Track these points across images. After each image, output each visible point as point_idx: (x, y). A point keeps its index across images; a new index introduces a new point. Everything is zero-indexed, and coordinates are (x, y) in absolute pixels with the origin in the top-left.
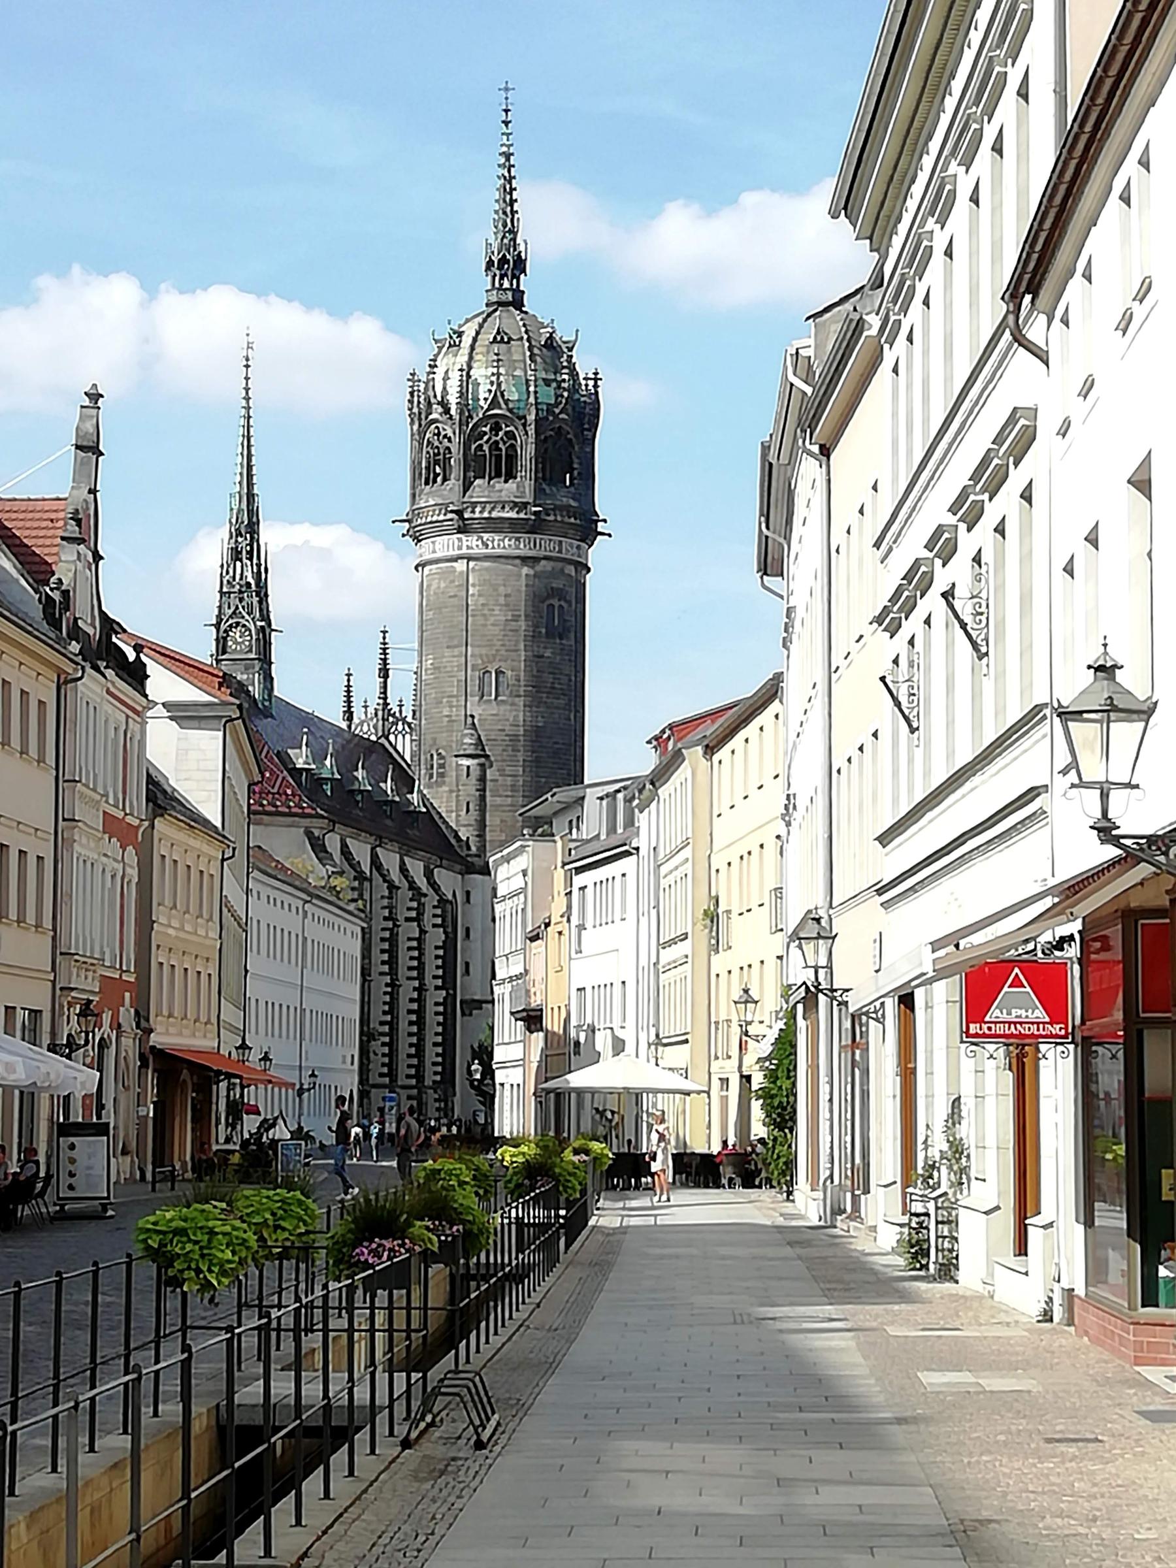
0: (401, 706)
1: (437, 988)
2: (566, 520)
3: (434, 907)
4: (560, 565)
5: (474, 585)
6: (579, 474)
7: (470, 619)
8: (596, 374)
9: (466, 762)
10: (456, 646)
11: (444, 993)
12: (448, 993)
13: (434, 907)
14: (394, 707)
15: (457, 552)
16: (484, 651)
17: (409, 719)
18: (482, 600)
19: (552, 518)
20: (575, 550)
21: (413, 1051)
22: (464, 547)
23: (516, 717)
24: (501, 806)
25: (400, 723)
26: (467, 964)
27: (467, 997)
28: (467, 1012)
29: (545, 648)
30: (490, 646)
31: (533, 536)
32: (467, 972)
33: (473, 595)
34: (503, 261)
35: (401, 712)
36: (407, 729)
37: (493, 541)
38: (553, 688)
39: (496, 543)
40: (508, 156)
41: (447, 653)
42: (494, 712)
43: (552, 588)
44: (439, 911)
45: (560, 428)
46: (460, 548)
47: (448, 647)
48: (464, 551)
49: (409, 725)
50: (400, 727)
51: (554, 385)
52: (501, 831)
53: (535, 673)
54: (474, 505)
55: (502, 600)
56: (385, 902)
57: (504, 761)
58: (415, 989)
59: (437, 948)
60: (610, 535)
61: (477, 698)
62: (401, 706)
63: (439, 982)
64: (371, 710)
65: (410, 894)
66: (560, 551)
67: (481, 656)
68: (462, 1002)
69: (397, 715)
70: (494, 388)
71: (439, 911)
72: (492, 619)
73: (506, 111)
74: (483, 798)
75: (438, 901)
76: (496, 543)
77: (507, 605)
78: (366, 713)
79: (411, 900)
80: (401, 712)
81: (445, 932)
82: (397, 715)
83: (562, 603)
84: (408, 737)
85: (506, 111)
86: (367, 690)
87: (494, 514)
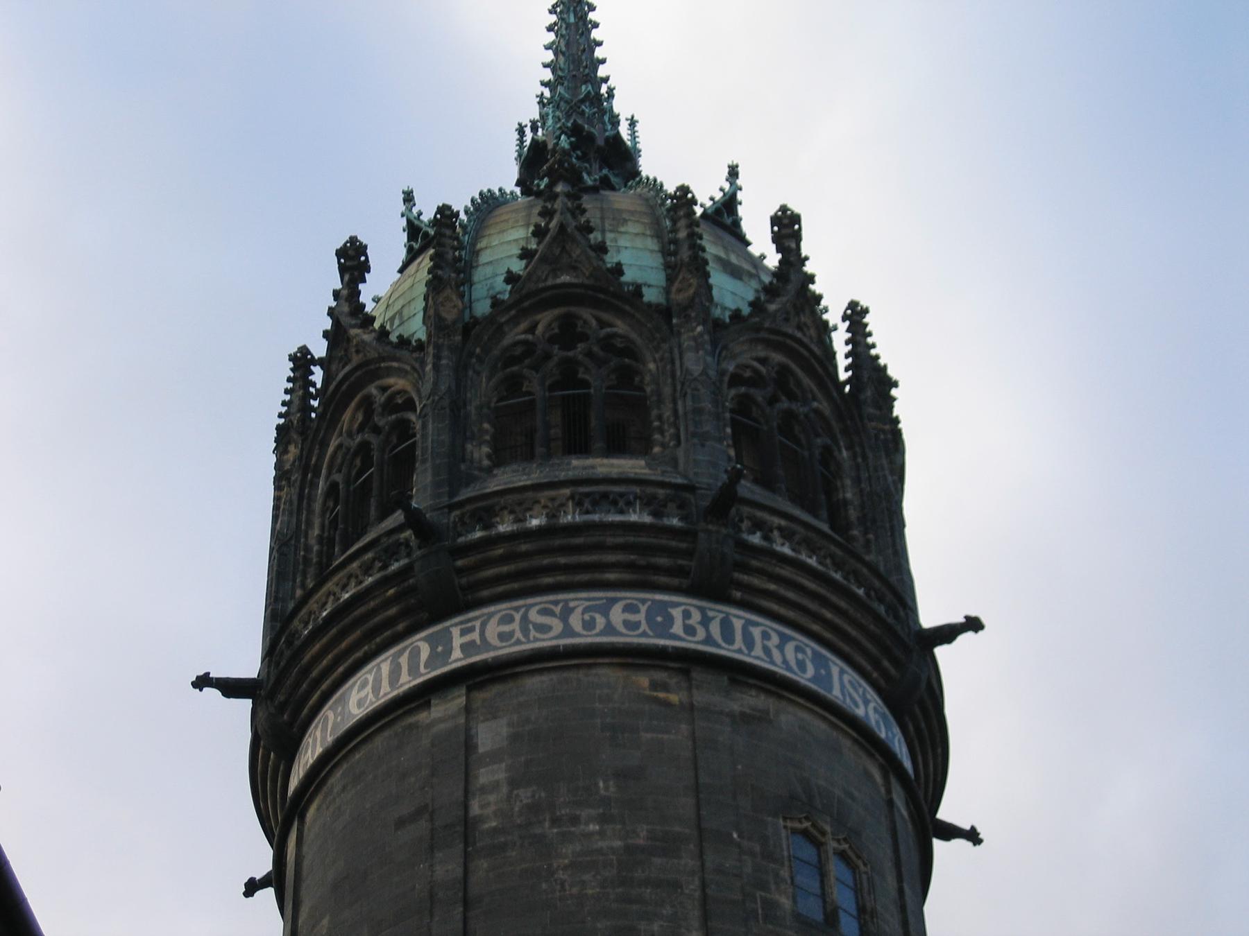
4: (819, 726)
5: (494, 757)
7: (482, 866)
15: (426, 675)
18: (525, 795)
19: (786, 550)
20: (871, 713)
22: (457, 653)
31: (718, 611)
33: (496, 786)
39: (575, 621)
45: (784, 371)
48: (457, 659)
54: (485, 513)
60: (973, 836)
66: (826, 680)
70: (553, 224)
76: (575, 621)
87: (570, 517)
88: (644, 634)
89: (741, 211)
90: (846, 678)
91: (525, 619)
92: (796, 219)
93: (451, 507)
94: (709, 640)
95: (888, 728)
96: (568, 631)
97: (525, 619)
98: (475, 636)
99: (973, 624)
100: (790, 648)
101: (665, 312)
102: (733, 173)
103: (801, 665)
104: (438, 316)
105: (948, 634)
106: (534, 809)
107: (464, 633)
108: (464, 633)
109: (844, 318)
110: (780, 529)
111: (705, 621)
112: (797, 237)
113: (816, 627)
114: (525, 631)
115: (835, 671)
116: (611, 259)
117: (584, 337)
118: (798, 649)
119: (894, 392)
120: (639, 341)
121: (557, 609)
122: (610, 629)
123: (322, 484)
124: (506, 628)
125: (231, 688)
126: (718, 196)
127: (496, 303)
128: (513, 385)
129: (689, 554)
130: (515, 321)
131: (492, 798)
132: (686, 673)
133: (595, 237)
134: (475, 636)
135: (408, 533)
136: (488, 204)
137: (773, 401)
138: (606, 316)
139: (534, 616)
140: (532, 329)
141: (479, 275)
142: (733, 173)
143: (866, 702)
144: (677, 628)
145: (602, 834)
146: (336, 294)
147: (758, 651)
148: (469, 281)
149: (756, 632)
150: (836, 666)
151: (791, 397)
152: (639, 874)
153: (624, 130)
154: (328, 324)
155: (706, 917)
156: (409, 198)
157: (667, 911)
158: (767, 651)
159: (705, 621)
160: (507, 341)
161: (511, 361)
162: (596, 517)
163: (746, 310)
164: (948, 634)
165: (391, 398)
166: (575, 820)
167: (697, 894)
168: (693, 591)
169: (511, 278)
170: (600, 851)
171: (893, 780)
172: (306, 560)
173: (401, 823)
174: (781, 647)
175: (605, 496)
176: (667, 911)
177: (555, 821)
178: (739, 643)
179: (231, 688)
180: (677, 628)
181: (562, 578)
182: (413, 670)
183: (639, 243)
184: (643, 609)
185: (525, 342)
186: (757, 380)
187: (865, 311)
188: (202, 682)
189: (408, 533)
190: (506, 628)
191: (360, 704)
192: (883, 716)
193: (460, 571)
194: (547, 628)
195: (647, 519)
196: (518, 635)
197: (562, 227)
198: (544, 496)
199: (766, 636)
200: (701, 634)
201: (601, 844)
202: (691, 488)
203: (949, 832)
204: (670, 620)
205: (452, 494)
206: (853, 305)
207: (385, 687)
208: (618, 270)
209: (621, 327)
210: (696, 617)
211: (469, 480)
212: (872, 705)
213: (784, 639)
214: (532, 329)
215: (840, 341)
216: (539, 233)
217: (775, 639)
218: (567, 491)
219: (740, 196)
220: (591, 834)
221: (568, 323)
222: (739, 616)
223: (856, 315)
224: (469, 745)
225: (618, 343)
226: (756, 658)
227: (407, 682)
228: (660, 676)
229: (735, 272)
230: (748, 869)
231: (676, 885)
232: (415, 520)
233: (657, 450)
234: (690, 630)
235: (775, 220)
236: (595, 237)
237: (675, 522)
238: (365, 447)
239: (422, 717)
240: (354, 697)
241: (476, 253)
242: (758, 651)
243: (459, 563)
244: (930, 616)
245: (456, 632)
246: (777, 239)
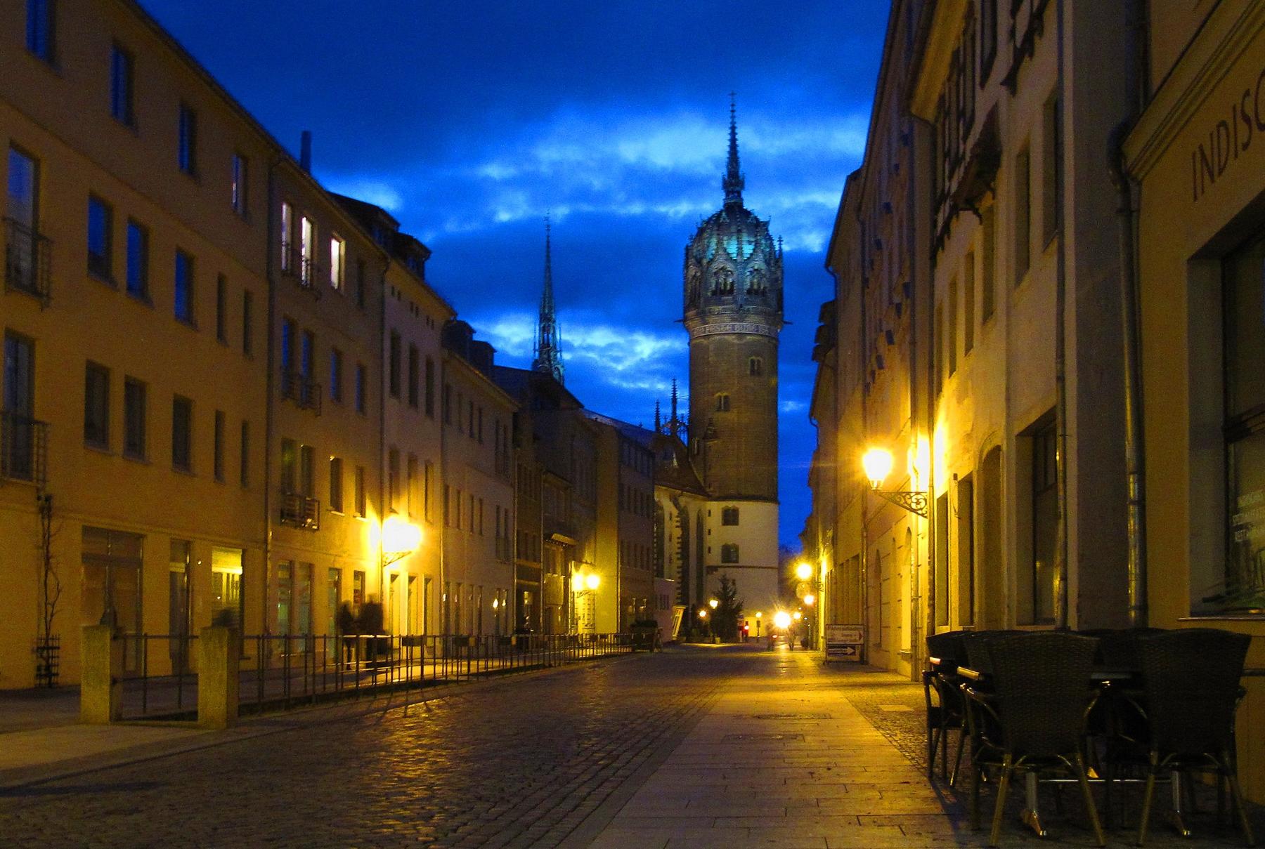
1: (678, 559)
3: (677, 517)
5: (711, 351)
8: (780, 238)
13: (677, 517)
14: (679, 417)
17: (686, 424)
26: (709, 549)
28: (710, 572)
32: (709, 551)
44: (678, 519)
46: (705, 332)
51: (754, 244)
59: (678, 538)
63: (679, 556)
64: (668, 420)
71: (678, 519)
73: (733, 105)
78: (666, 421)
80: (682, 420)
81: (682, 529)
83: (759, 358)
85: (733, 105)
86: (666, 411)
224: (708, 349)
228: (734, 337)
229: (750, 243)
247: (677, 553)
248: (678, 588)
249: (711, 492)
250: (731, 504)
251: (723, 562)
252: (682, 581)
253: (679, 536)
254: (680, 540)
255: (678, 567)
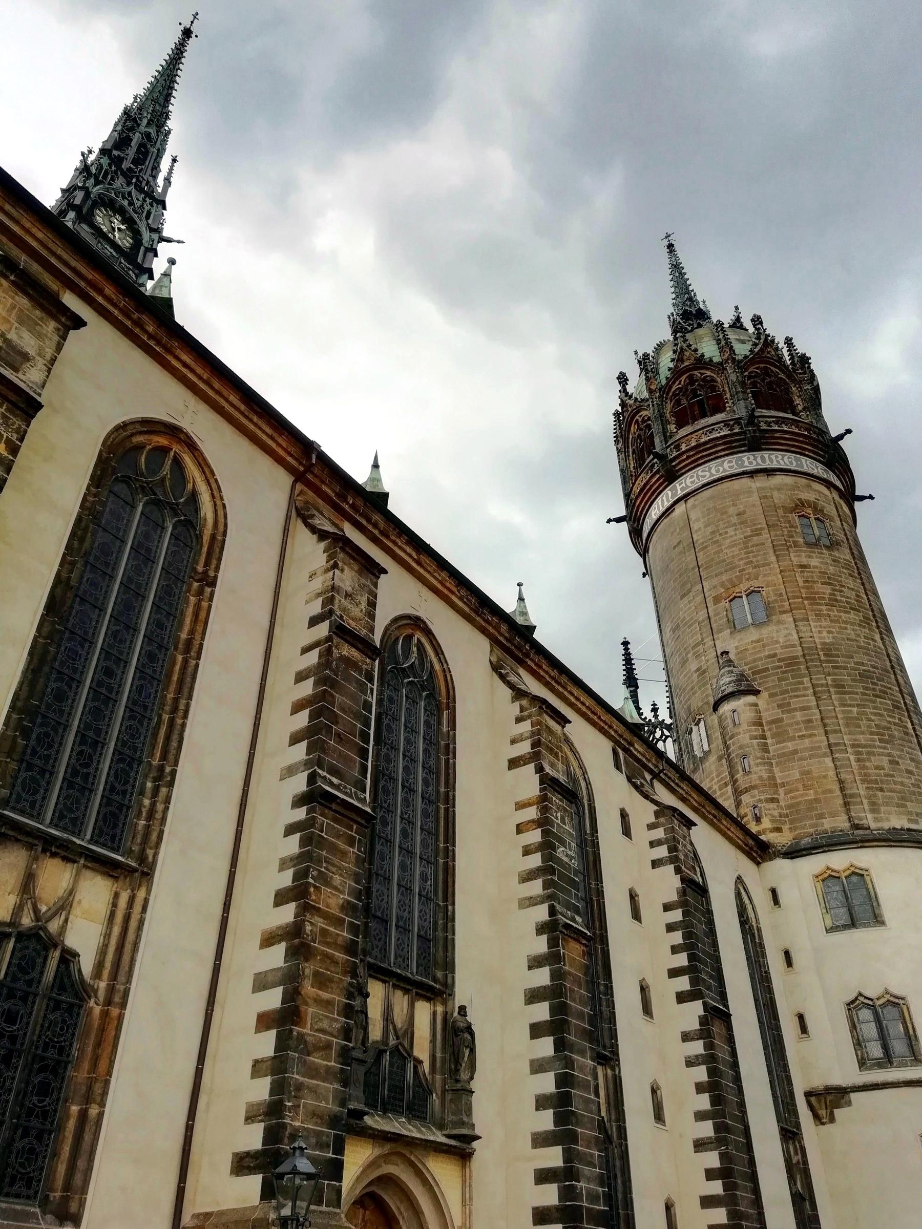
0: (655, 710)
1: (681, 998)
2: (797, 431)
3: (651, 827)
4: (803, 481)
5: (698, 520)
6: (804, 409)
7: (701, 555)
9: (726, 708)
10: (689, 591)
11: (696, 1008)
12: (705, 1005)
13: (651, 827)
15: (672, 501)
16: (724, 578)
17: (668, 721)
18: (710, 529)
19: (776, 428)
21: (546, 1121)
22: (679, 492)
23: (790, 634)
24: (796, 752)
25: (658, 730)
27: (819, 1082)
28: (822, 1112)
29: (810, 557)
30: (732, 569)
31: (758, 454)
32: (804, 1029)
33: (700, 529)
34: (686, 315)
35: (656, 716)
36: (666, 733)
37: (710, 469)
38: (836, 600)
39: (713, 471)
40: (677, 268)
41: (683, 603)
42: (754, 638)
43: (800, 500)
44: (659, 833)
47: (683, 597)
48: (680, 493)
49: (669, 727)
50: (658, 734)
52: (806, 787)
53: (801, 584)
55: (734, 520)
56: (318, 584)
57: (787, 692)
58: (541, 929)
59: (667, 907)
61: (729, 631)
62: (655, 710)
63: (683, 983)
65: (515, 709)
67: (722, 584)
68: (808, 1095)
69: (653, 720)
71: (659, 833)
72: (729, 541)
74: (765, 748)
75: (657, 814)
76: (713, 471)
77: (742, 523)
79: (519, 720)
80: (656, 716)
81: (678, 871)
82: (653, 720)
84: (669, 739)
88: (736, 469)
89: (742, 320)
90: (808, 462)
91: (697, 474)
92: (759, 318)
93: (667, 448)
94: (758, 464)
95: (827, 473)
96: (712, 475)
97: (698, 476)
98: (684, 485)
99: (849, 431)
100: (786, 458)
101: (721, 364)
102: (737, 308)
103: (791, 463)
104: (650, 388)
105: (841, 437)
106: (713, 533)
107: (680, 485)
108: (680, 485)
109: (785, 343)
110: (773, 421)
111: (755, 459)
112: (761, 323)
113: (793, 449)
114: (698, 479)
115: (803, 461)
116: (700, 353)
117: (697, 380)
118: (788, 458)
119: (810, 361)
120: (715, 376)
121: (707, 469)
122: (725, 470)
123: (631, 450)
124: (692, 480)
125: (618, 520)
126: (733, 318)
127: (667, 378)
128: (678, 403)
129: (744, 440)
130: (674, 383)
131: (699, 533)
132: (752, 477)
133: (693, 348)
134: (684, 485)
135: (656, 460)
136: (660, 347)
137: (763, 380)
138: (701, 371)
139: (700, 473)
140: (680, 383)
141: (660, 371)
142: (737, 308)
143: (817, 468)
144: (746, 464)
145: (736, 534)
146: (620, 391)
147: (775, 463)
148: (658, 374)
149: (773, 457)
150: (803, 459)
151: (770, 376)
152: (750, 544)
153: (701, 306)
154: (619, 401)
155: (775, 552)
156: (636, 353)
157: (762, 552)
158: (778, 462)
159: (755, 459)
160: (673, 389)
161: (675, 395)
162: (711, 437)
163: (748, 353)
164: (841, 437)
165: (643, 418)
166: (726, 533)
167: (771, 545)
168: (750, 450)
169: (670, 369)
170: (736, 540)
171: (832, 489)
172: (632, 475)
173: (674, 548)
174: (783, 459)
175: (713, 429)
176: (762, 552)
177: (720, 535)
178: (768, 462)
179: (618, 520)
180: (746, 464)
181: (706, 459)
182: (668, 501)
183: (709, 343)
184: (734, 461)
185: (679, 388)
186: (757, 375)
187: (791, 339)
188: (609, 521)
189: (656, 460)
190: (692, 480)
191: (655, 514)
192: (825, 470)
193: (675, 466)
194: (704, 476)
195: (729, 432)
196: (697, 481)
197: (682, 348)
198: (694, 436)
199: (777, 457)
200: (755, 463)
201: (735, 538)
202: (741, 418)
203: (861, 498)
204: (743, 462)
205: (666, 444)
206: (787, 338)
207: (661, 508)
208: (703, 355)
209: (708, 373)
210: (752, 458)
211: (671, 437)
212: (819, 468)
213: (783, 456)
214: (680, 383)
215: (785, 352)
216: (675, 352)
217: (780, 457)
218: (701, 432)
219: (740, 315)
220: (732, 536)
221: (691, 377)
222: (766, 454)
223: (789, 342)
225: (708, 379)
226: (775, 465)
227: (667, 504)
229: (743, 342)
230: (786, 533)
231: (763, 544)
232: (656, 455)
233: (728, 409)
234: (751, 463)
235: (752, 320)
236: (693, 348)
237: (737, 430)
238: (639, 435)
239: (673, 515)
240: (653, 513)
241: (658, 364)
242: (775, 463)
243: (674, 464)
244: (834, 434)
245: (677, 485)
246: (754, 326)
247: (674, 973)
248: (700, 1145)
249: (764, 831)
250: (839, 860)
251: (863, 1063)
252: (715, 1101)
253: (674, 897)
254: (676, 915)
255: (686, 1037)
